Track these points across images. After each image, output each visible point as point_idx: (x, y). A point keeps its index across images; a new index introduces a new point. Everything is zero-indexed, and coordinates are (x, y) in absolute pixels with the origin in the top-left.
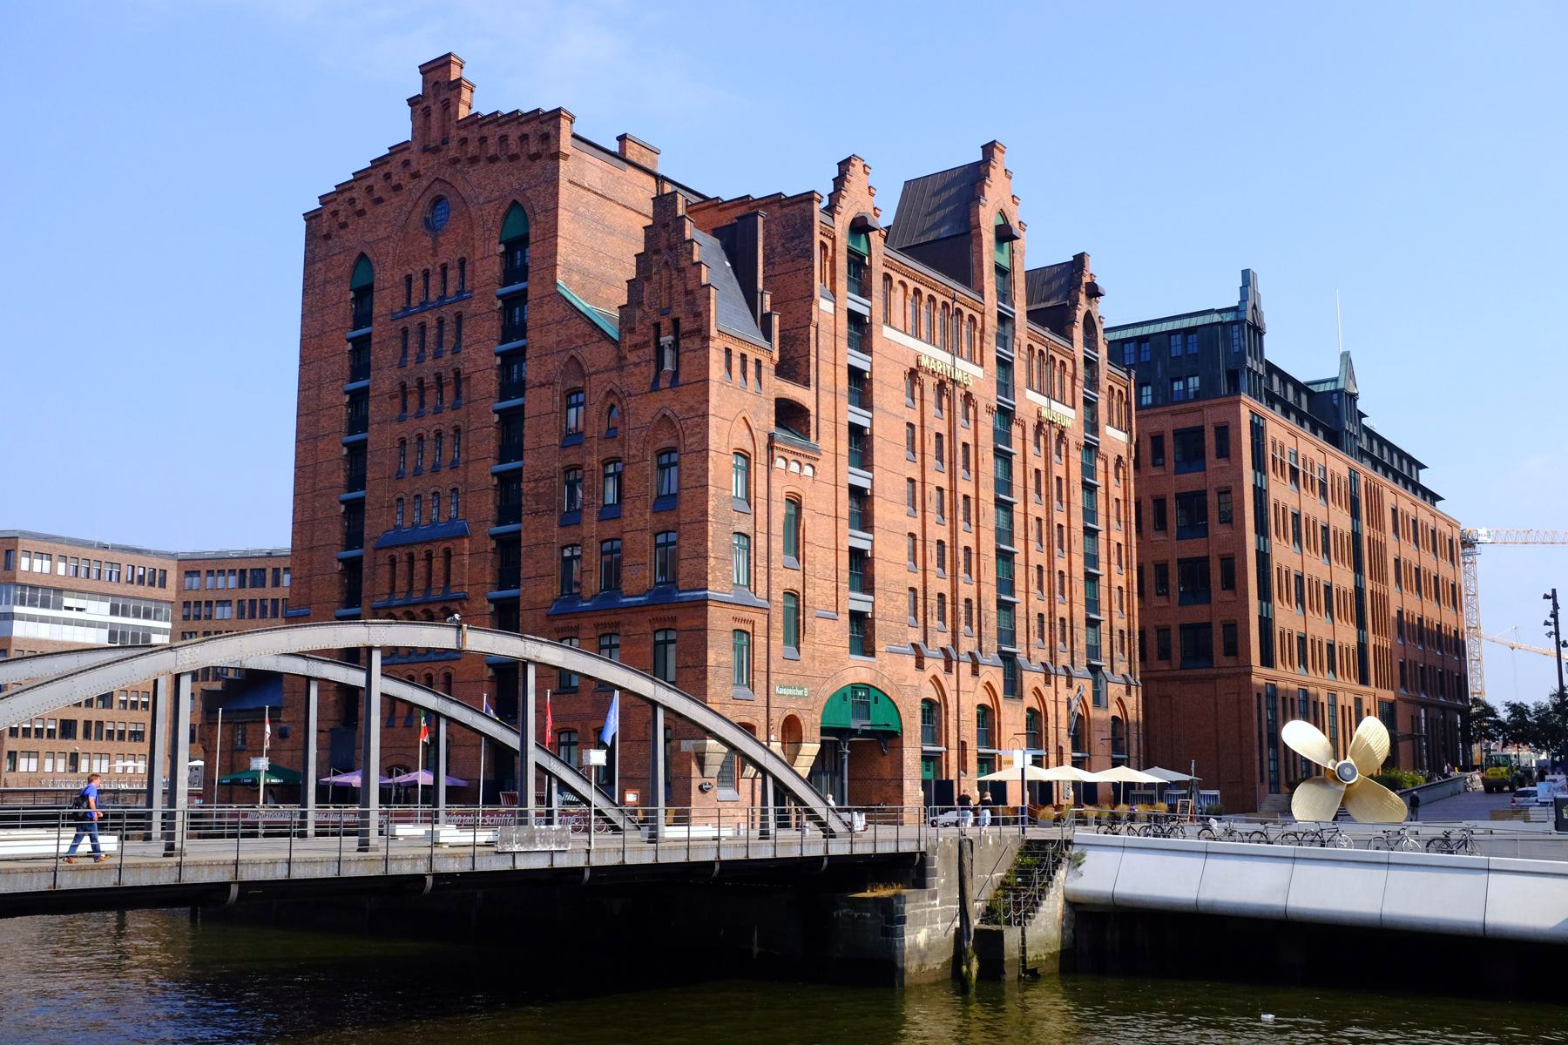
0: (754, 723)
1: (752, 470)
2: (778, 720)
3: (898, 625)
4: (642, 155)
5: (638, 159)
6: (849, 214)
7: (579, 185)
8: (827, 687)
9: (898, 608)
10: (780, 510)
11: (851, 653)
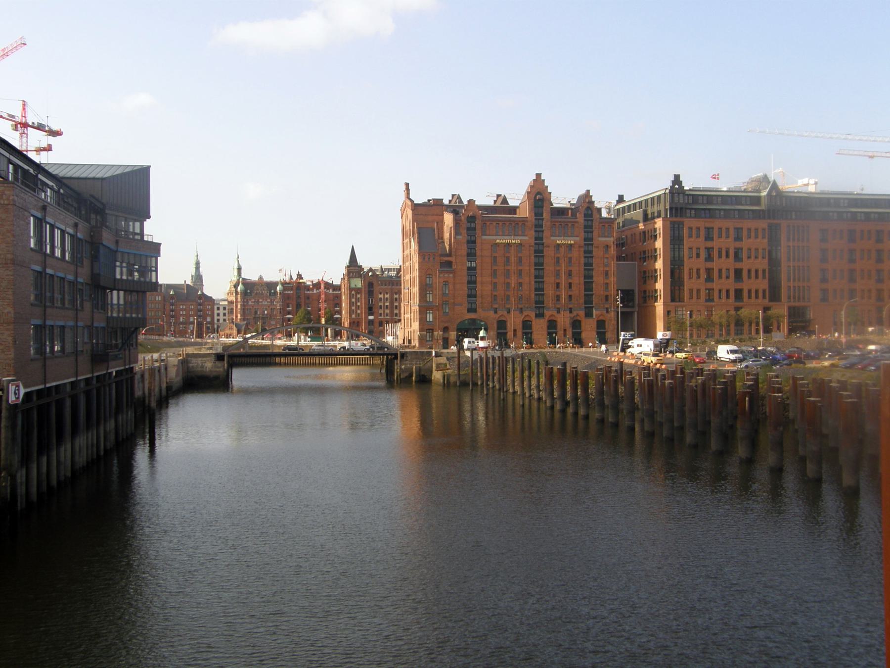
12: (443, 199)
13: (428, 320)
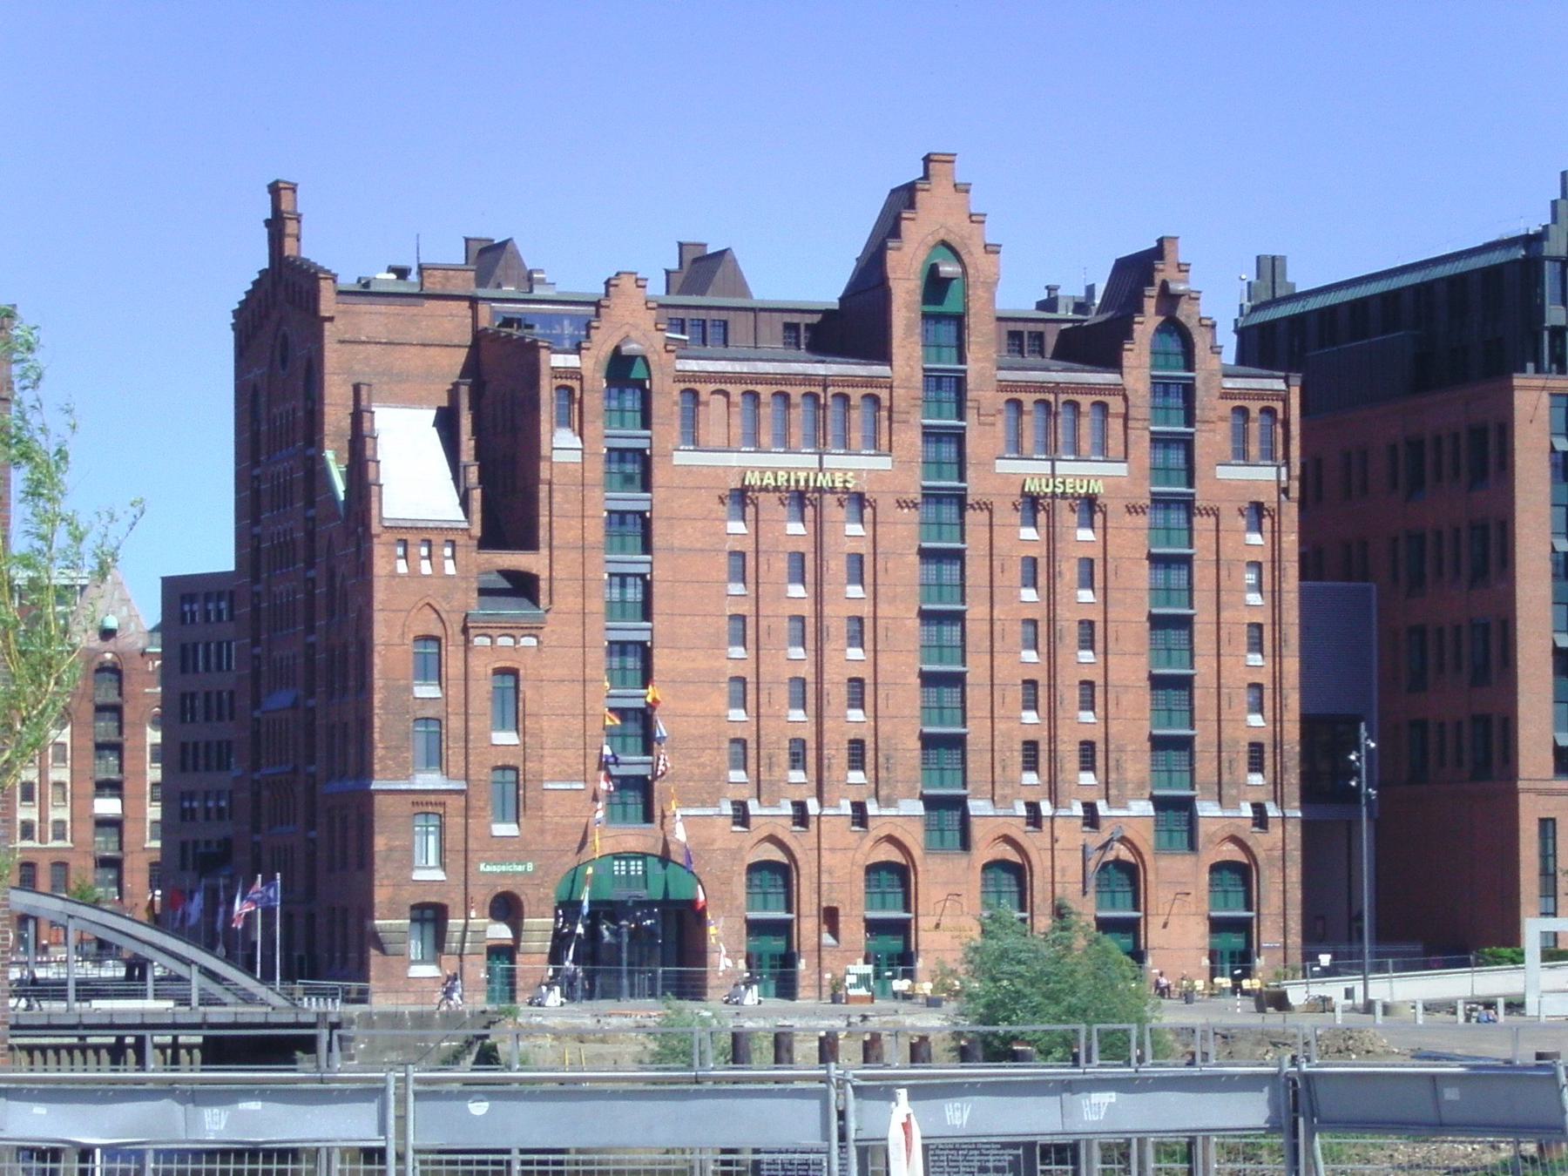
0: (445, 901)
1: (444, 653)
2: (482, 896)
4: (448, 279)
5: (443, 286)
6: (610, 342)
8: (566, 859)
9: (703, 765)
10: (483, 687)
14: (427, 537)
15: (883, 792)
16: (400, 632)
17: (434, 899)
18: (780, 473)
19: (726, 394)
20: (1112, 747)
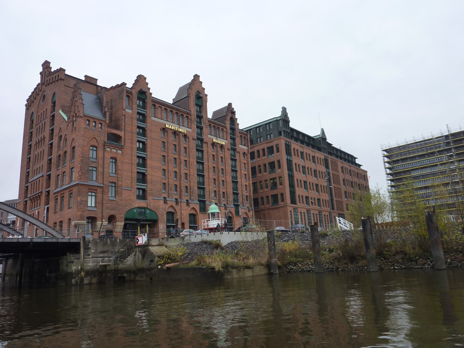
0: (97, 216)
2: (106, 215)
3: (157, 192)
4: (91, 80)
7: (68, 87)
11: (137, 199)
12: (97, 80)
13: (89, 205)
14: (95, 121)
15: (192, 198)
16: (87, 143)
17: (93, 216)
18: (172, 127)
19: (161, 107)
20: (228, 193)
